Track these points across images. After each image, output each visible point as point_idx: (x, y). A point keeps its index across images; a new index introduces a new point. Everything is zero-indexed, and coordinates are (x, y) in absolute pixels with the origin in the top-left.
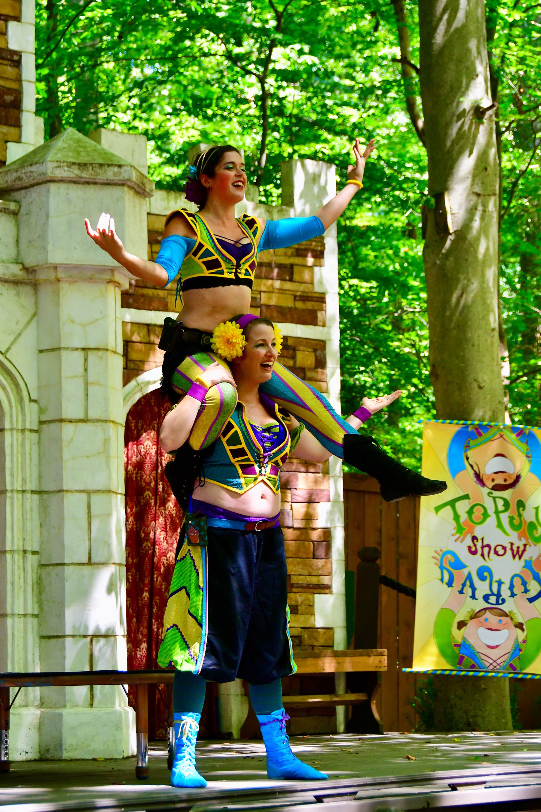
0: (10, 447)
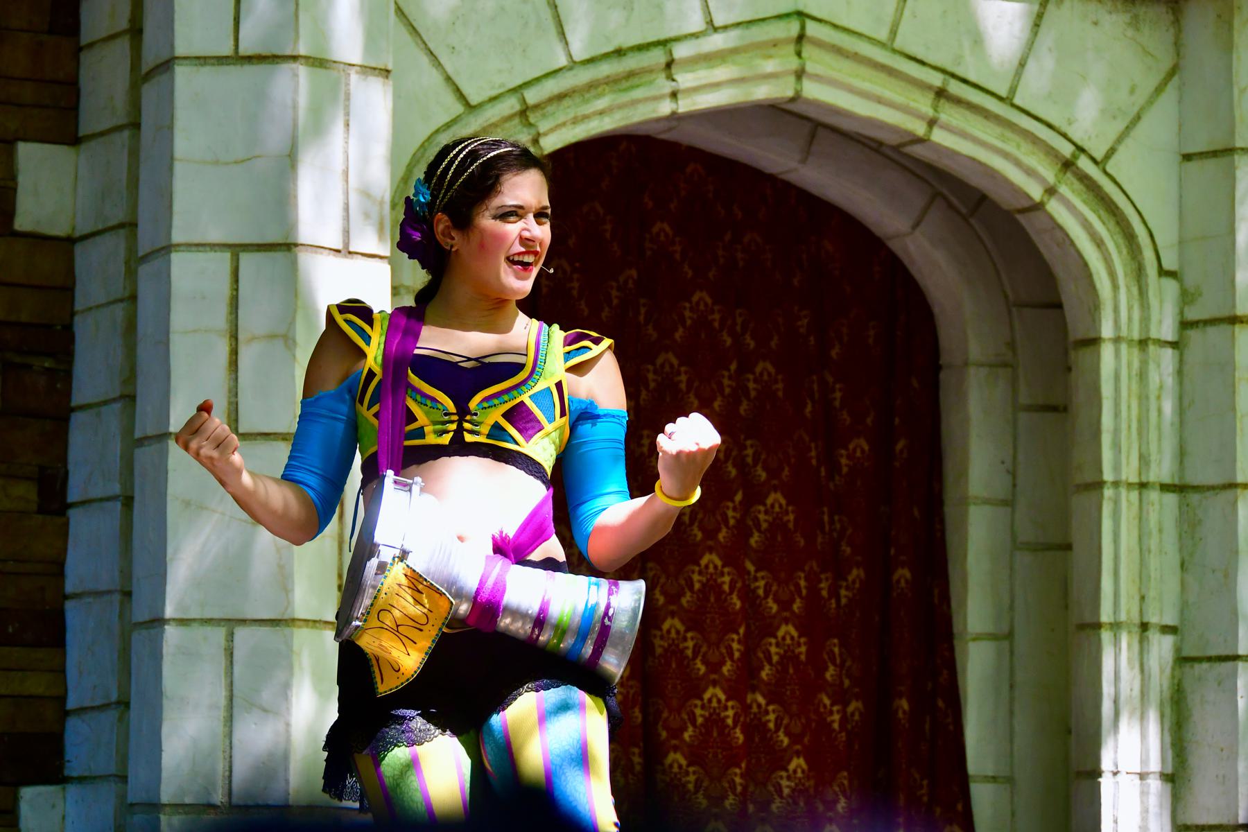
0: (1112, 382)
